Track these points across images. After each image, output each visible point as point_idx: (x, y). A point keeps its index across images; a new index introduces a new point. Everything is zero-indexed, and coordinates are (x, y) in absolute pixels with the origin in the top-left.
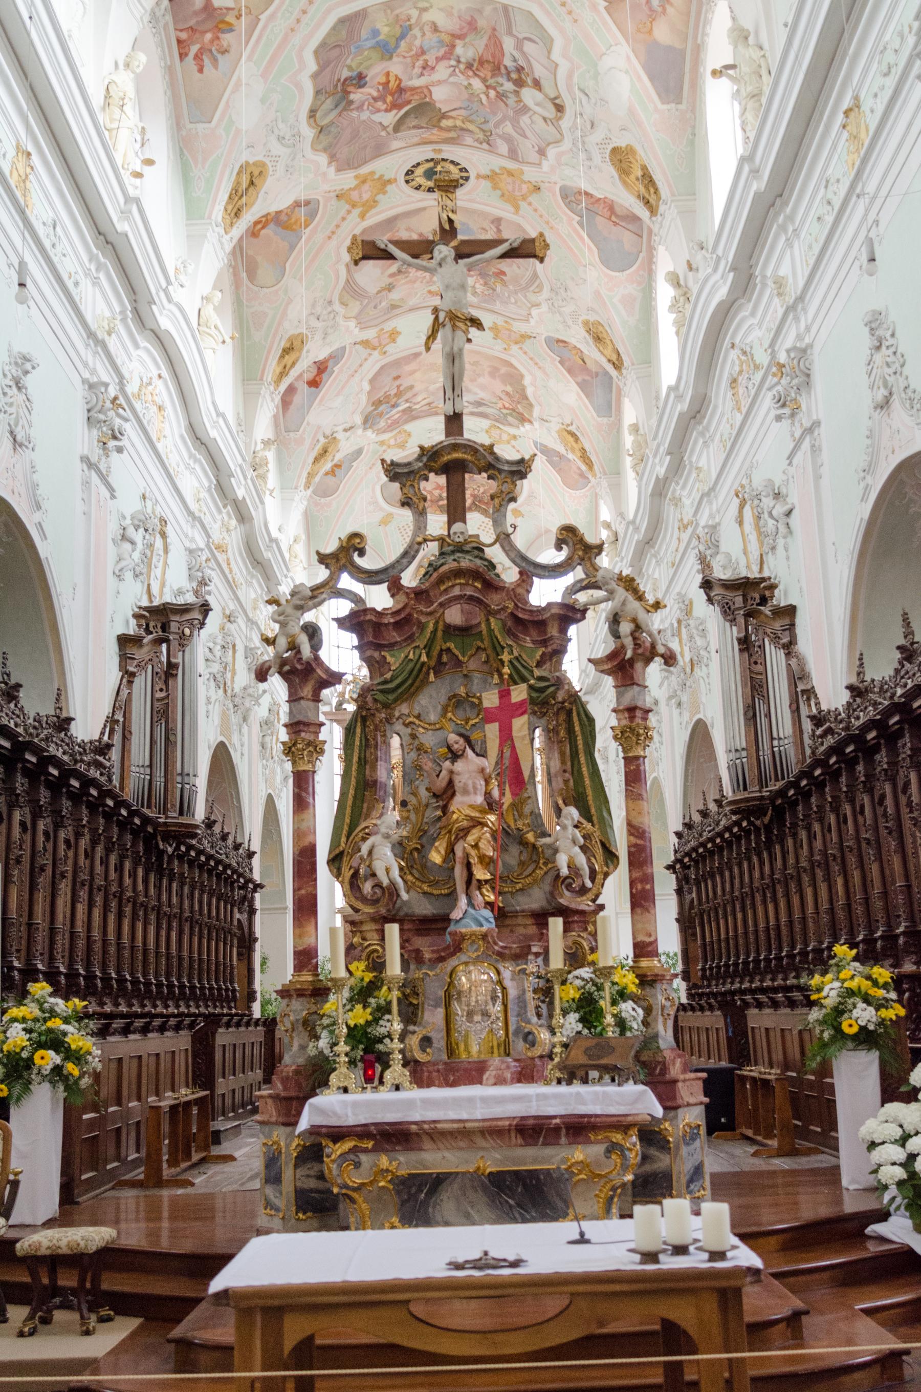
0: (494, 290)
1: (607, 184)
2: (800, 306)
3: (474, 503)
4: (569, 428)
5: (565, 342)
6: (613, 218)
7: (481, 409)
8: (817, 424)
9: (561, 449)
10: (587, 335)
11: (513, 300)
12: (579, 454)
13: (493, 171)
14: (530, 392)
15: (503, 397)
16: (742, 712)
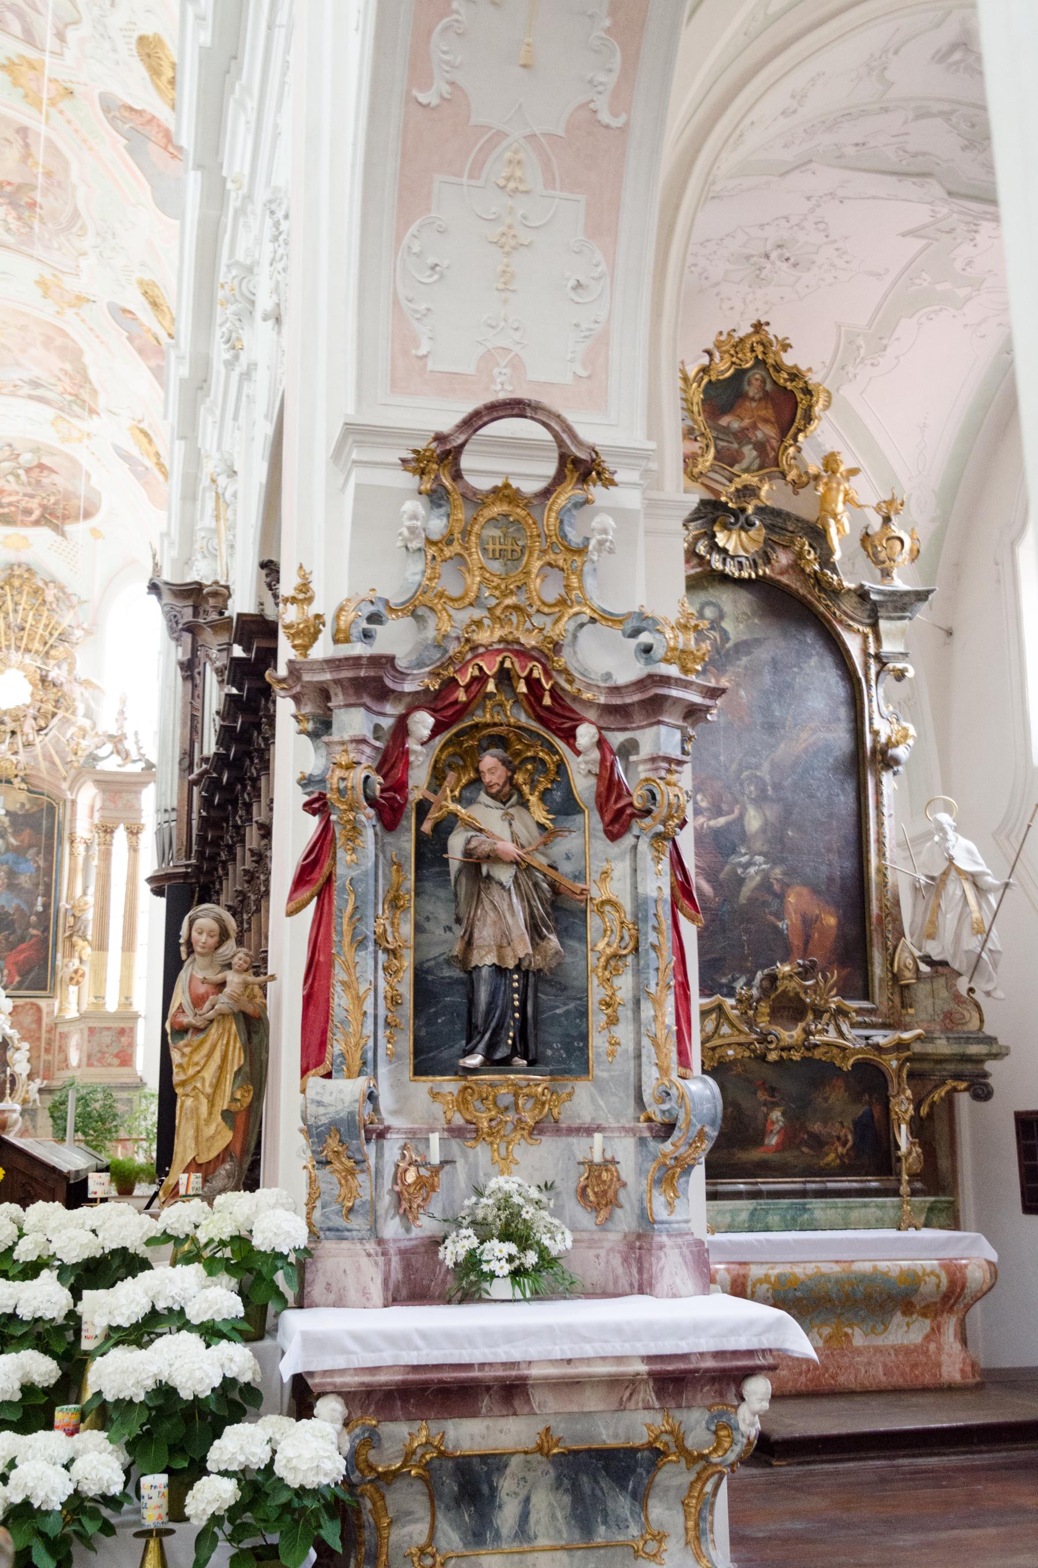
0: (31, 228)
1: (137, 90)
2: (250, 208)
3: (43, 516)
4: (141, 426)
5: (130, 312)
6: (171, 149)
7: (39, 392)
8: (252, 366)
9: (135, 451)
10: (142, 299)
11: (56, 245)
12: (155, 460)
13: (9, 59)
14: (92, 373)
15: (62, 377)
16: (177, 760)
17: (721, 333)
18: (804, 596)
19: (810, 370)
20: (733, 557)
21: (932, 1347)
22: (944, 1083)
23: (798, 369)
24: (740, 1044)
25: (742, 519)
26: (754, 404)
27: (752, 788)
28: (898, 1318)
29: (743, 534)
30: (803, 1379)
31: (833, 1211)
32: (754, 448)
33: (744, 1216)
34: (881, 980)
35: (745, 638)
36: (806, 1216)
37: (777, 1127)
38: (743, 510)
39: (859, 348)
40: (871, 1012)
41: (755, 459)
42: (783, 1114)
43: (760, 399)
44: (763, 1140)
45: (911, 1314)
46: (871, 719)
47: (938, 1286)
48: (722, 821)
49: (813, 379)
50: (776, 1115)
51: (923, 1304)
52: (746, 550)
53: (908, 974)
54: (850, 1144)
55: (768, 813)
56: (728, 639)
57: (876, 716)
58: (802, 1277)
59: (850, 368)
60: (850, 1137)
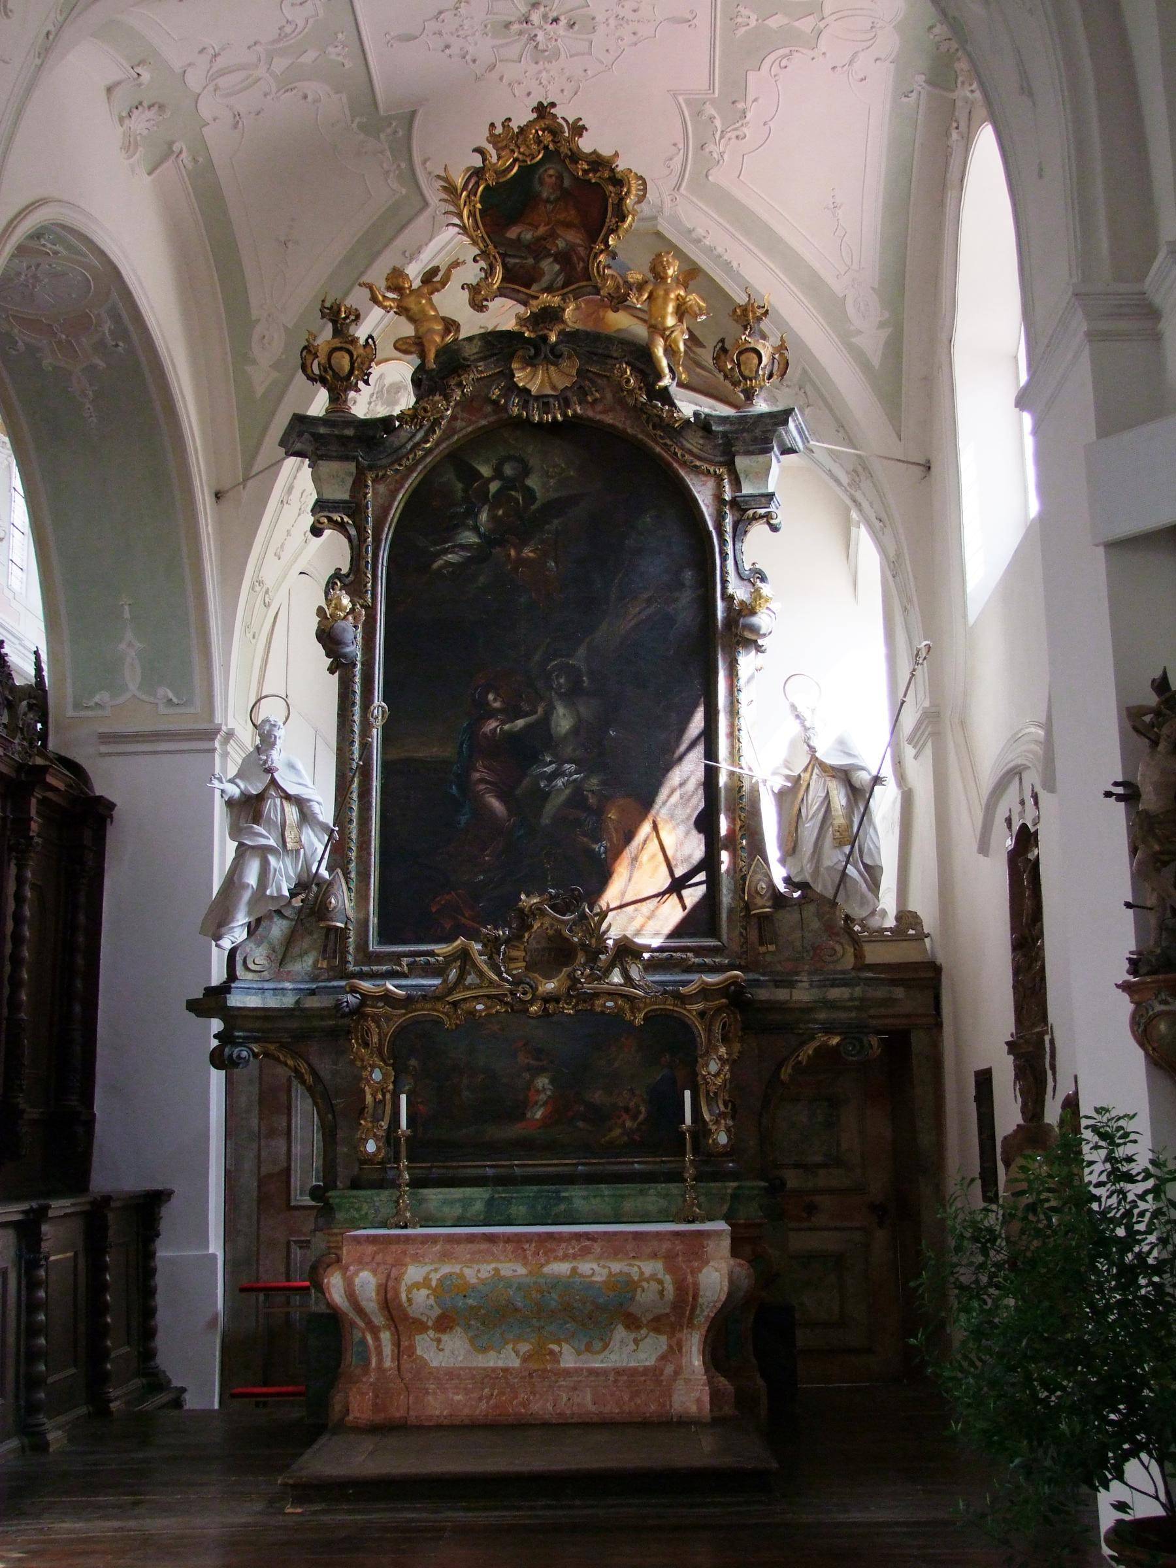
17: (492, 125)
18: (635, 437)
19: (616, 154)
20: (537, 398)
21: (669, 1369)
22: (812, 1038)
23: (599, 156)
24: (488, 997)
25: (545, 350)
26: (550, 207)
27: (562, 681)
28: (620, 1333)
29: (552, 368)
30: (483, 1405)
31: (598, 1200)
32: (556, 261)
33: (479, 1206)
34: (731, 910)
35: (556, 495)
36: (562, 1207)
37: (543, 1097)
38: (545, 339)
39: (712, 118)
40: (715, 951)
41: (558, 274)
42: (552, 1081)
43: (557, 200)
44: (524, 1114)
45: (639, 1327)
46: (724, 582)
47: (661, 1293)
48: (520, 723)
49: (621, 165)
50: (542, 1081)
51: (650, 1316)
52: (554, 388)
53: (759, 901)
54: (641, 1117)
55: (582, 710)
56: (535, 499)
57: (732, 577)
58: (474, 1281)
59: (710, 147)
60: (643, 1109)
